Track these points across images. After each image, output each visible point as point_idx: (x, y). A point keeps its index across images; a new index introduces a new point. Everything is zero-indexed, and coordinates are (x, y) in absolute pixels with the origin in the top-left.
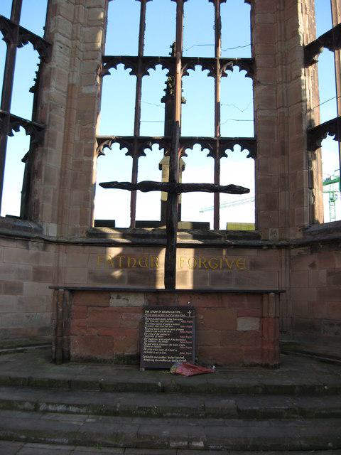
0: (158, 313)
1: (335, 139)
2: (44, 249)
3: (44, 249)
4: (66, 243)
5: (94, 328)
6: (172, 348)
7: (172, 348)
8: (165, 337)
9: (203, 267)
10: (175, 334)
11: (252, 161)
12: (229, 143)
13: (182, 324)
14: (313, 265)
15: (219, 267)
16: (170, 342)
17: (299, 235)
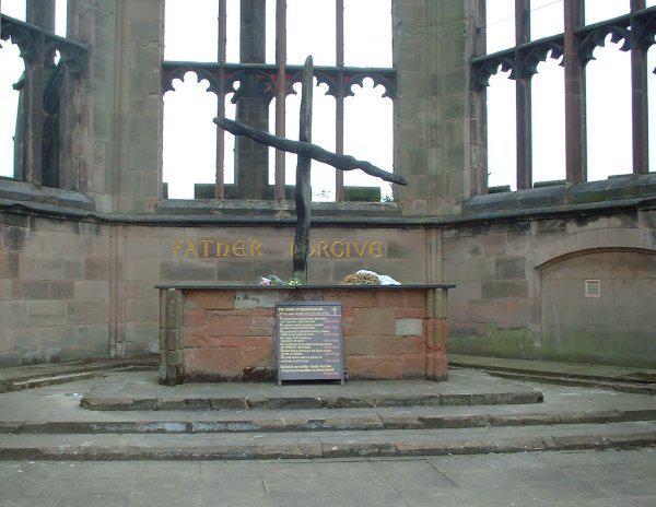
0: (295, 312)
1: (511, 77)
2: (97, 232)
3: (97, 232)
4: (126, 223)
5: (216, 337)
6: (313, 354)
7: (313, 354)
8: (306, 341)
9: (323, 255)
10: (318, 338)
11: (389, 102)
12: (357, 75)
13: (327, 324)
14: (475, 251)
15: (345, 256)
16: (312, 347)
17: (457, 210)
